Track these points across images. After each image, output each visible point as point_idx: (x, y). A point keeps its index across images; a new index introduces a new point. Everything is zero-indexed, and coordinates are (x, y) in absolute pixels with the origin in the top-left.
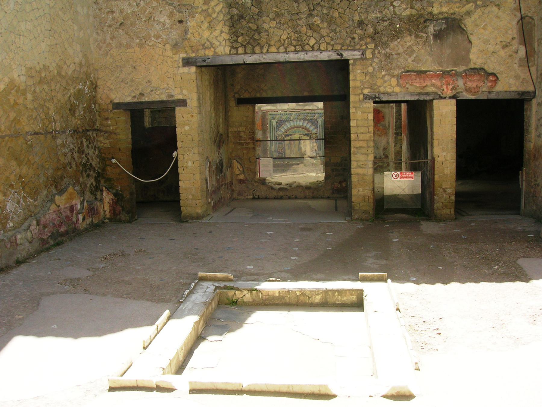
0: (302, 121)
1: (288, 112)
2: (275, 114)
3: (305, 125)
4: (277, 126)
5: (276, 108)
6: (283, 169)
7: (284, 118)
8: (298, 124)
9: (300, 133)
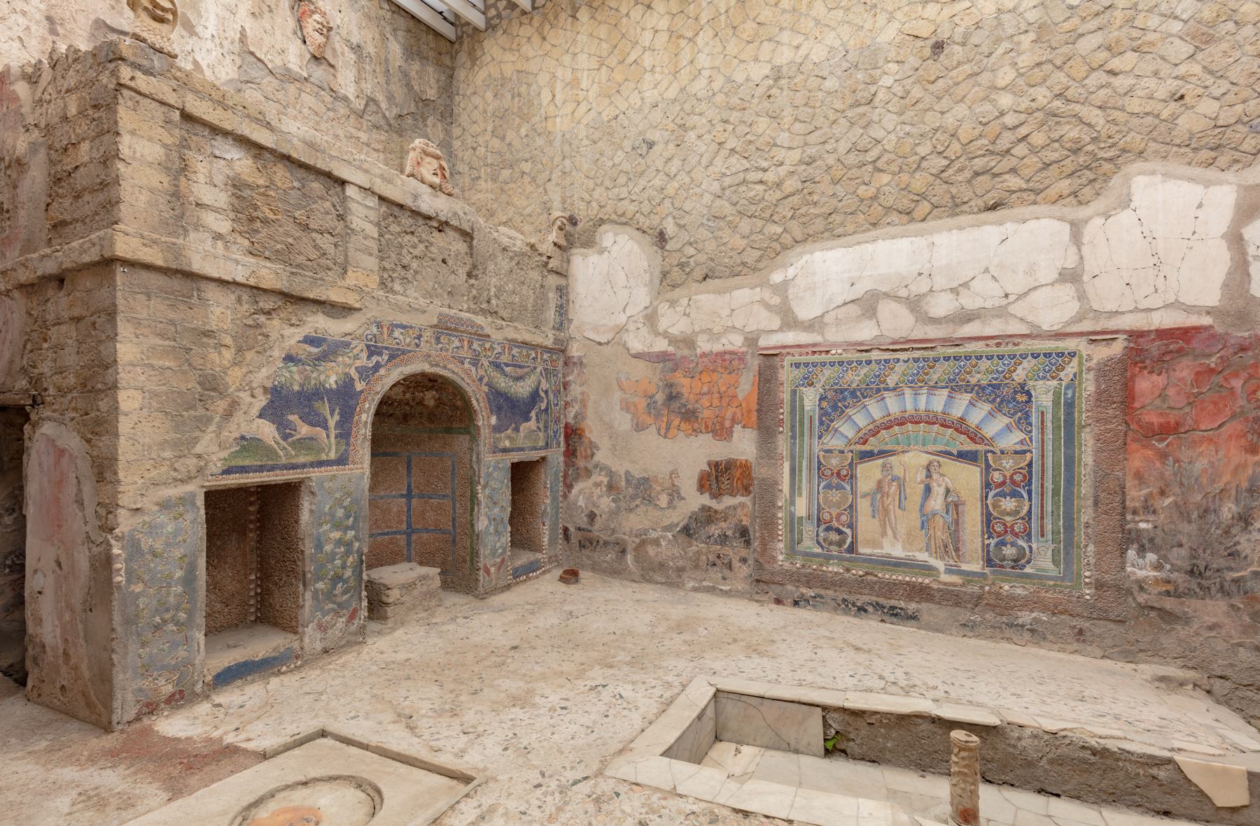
0: (945, 392)
1: (875, 355)
2: (814, 365)
3: (957, 411)
4: (823, 412)
5: (819, 339)
6: (844, 600)
7: (854, 378)
8: (922, 406)
9: (931, 448)
